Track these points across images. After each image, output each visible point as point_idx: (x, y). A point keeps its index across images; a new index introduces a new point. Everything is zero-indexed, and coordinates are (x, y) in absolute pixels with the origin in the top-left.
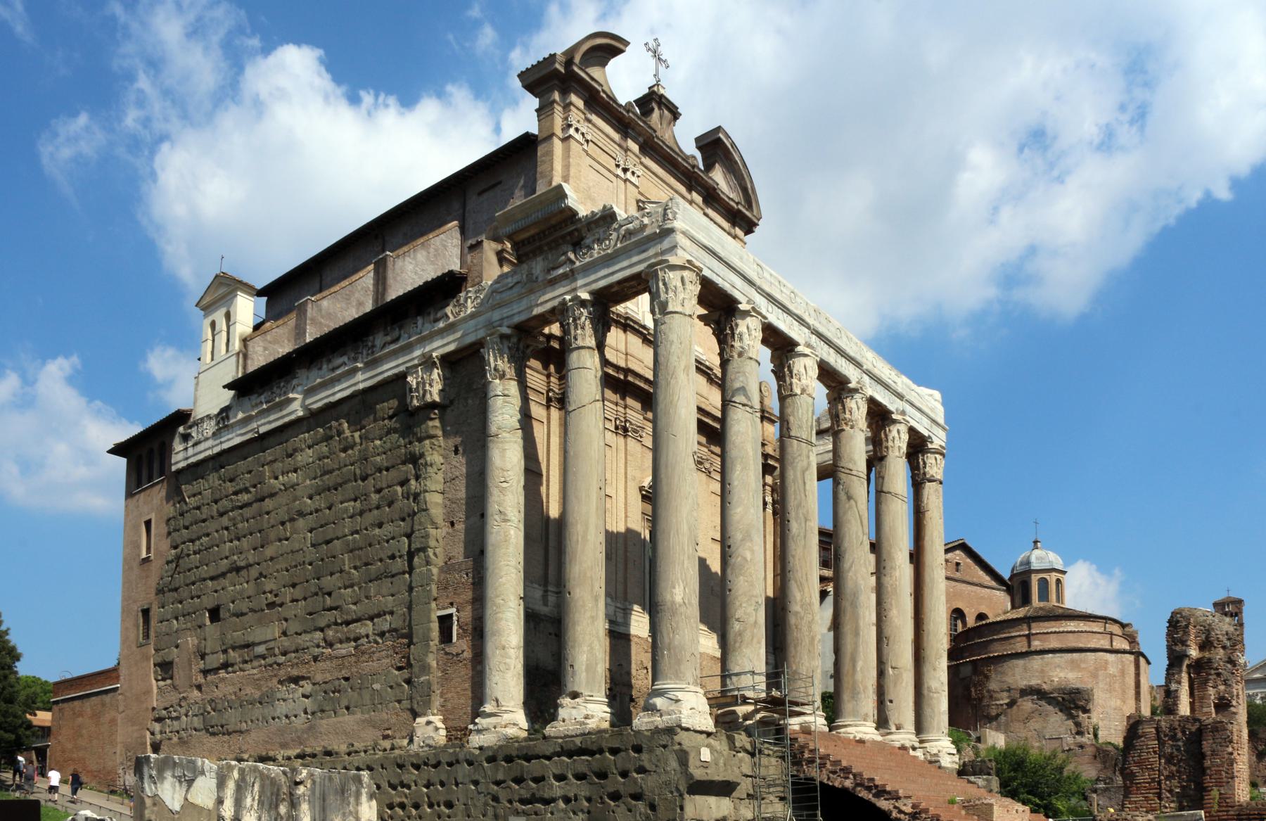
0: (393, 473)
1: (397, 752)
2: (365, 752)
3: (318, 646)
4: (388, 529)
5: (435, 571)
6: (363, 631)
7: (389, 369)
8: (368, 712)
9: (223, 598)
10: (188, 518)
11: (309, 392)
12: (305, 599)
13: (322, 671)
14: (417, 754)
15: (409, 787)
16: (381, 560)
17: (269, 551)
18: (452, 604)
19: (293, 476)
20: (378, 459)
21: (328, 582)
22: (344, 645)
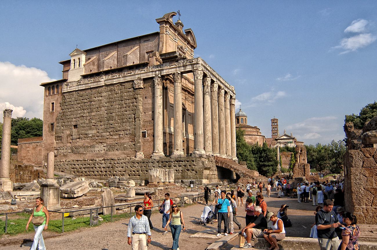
0: (130, 101)
1: (132, 160)
2: (123, 160)
3: (108, 136)
4: (128, 113)
5: (141, 122)
6: (121, 133)
8: (123, 151)
9: (78, 123)
10: (67, 104)
12: (104, 125)
13: (109, 142)
14: (138, 160)
15: (136, 167)
16: (126, 119)
17: (93, 114)
18: (146, 129)
20: (125, 97)
21: (111, 122)
22: (116, 136)
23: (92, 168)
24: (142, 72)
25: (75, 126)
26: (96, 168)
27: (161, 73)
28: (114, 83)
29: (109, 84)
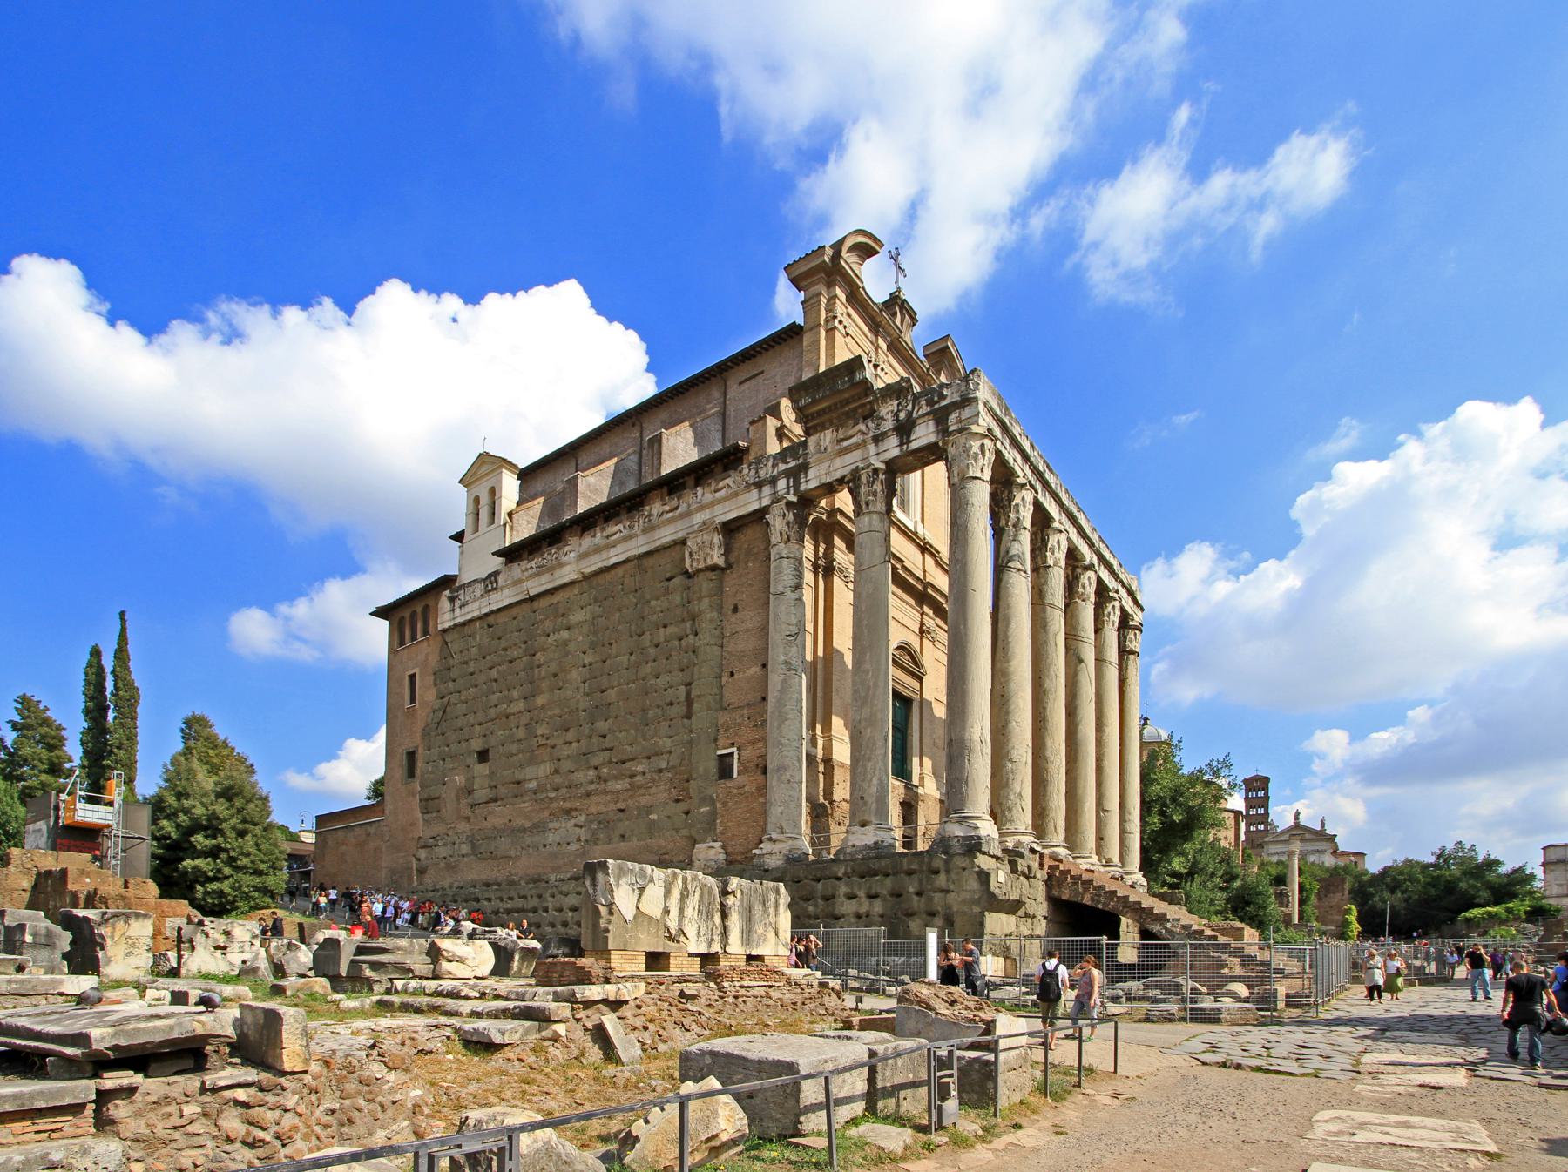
0: (671, 630)
7: (666, 535)
9: (493, 741)
11: (583, 556)
19: (565, 634)
23: (535, 911)
24: (718, 495)
25: (483, 756)
26: (546, 910)
27: (797, 484)
28: (614, 561)
29: (594, 568)
